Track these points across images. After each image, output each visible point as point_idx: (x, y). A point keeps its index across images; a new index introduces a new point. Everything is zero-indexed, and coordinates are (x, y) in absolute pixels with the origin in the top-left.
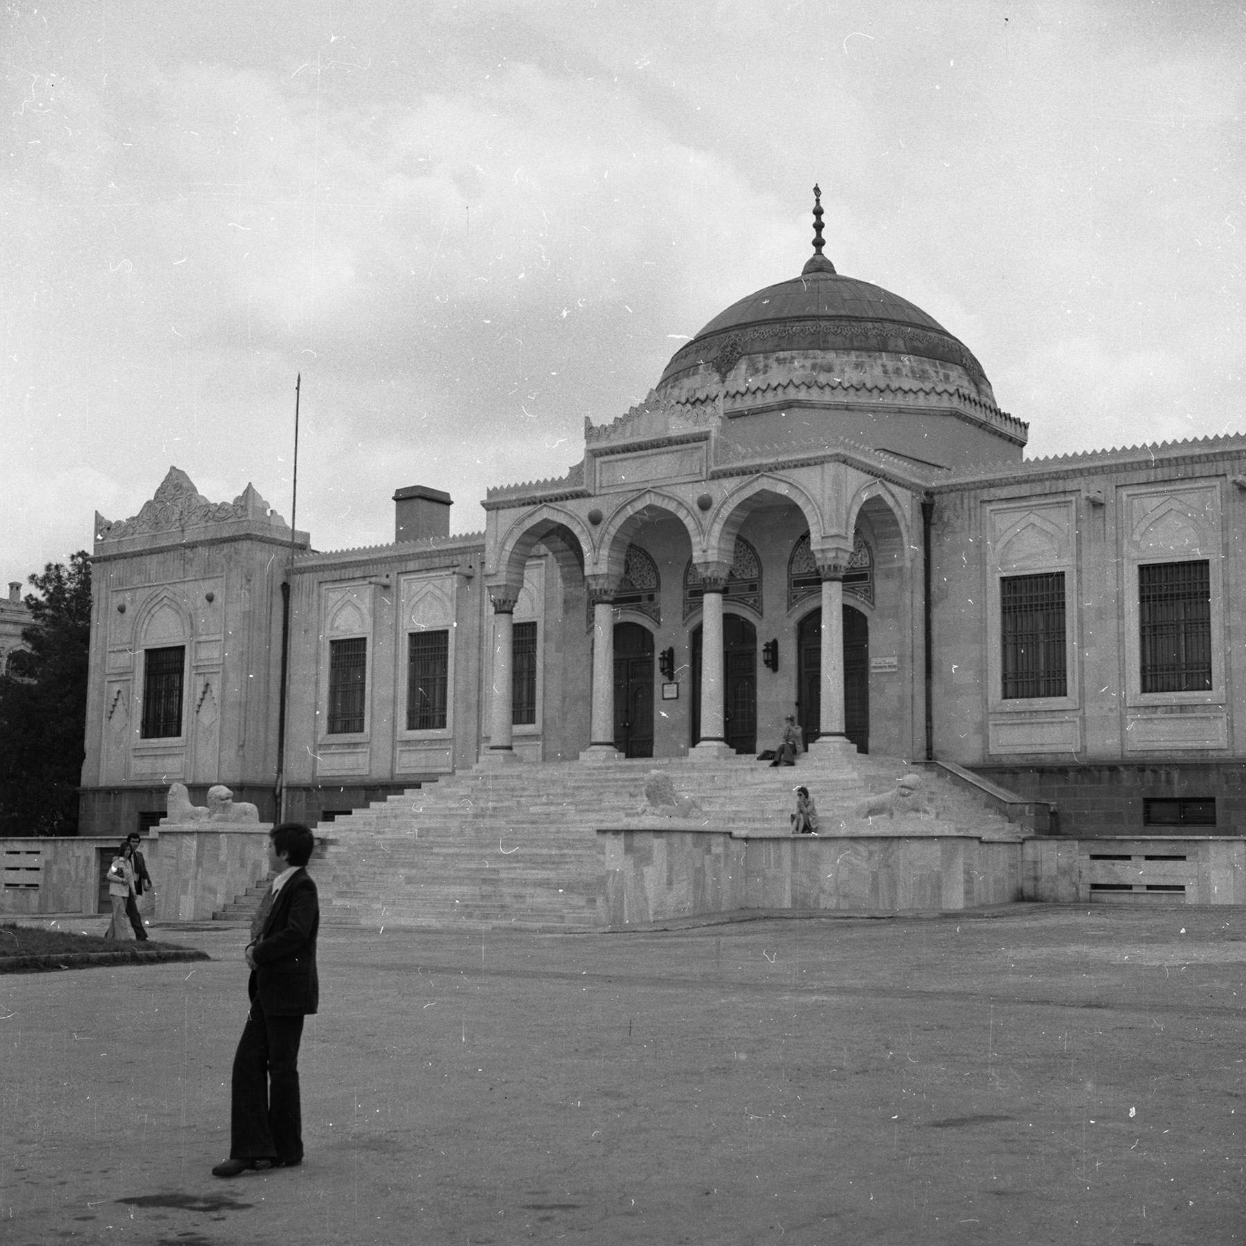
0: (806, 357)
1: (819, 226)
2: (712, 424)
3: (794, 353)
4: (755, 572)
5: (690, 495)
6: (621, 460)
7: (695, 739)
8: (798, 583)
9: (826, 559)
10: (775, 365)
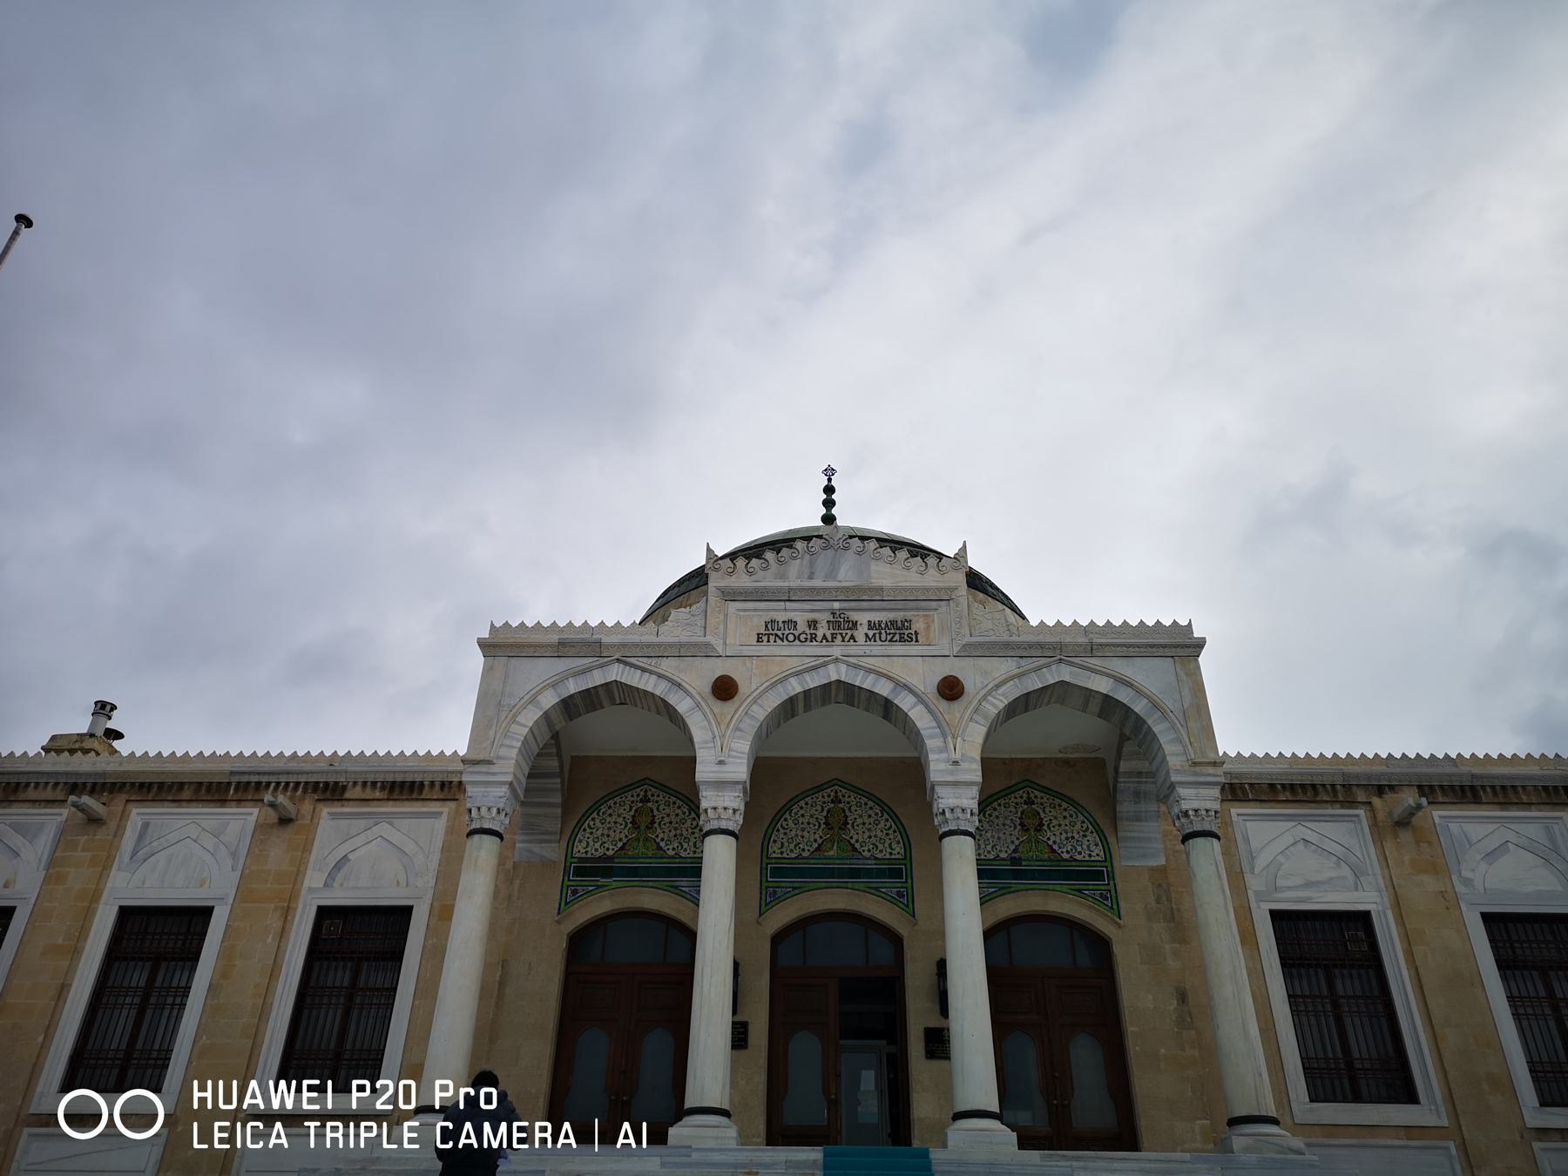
4: (898, 849)
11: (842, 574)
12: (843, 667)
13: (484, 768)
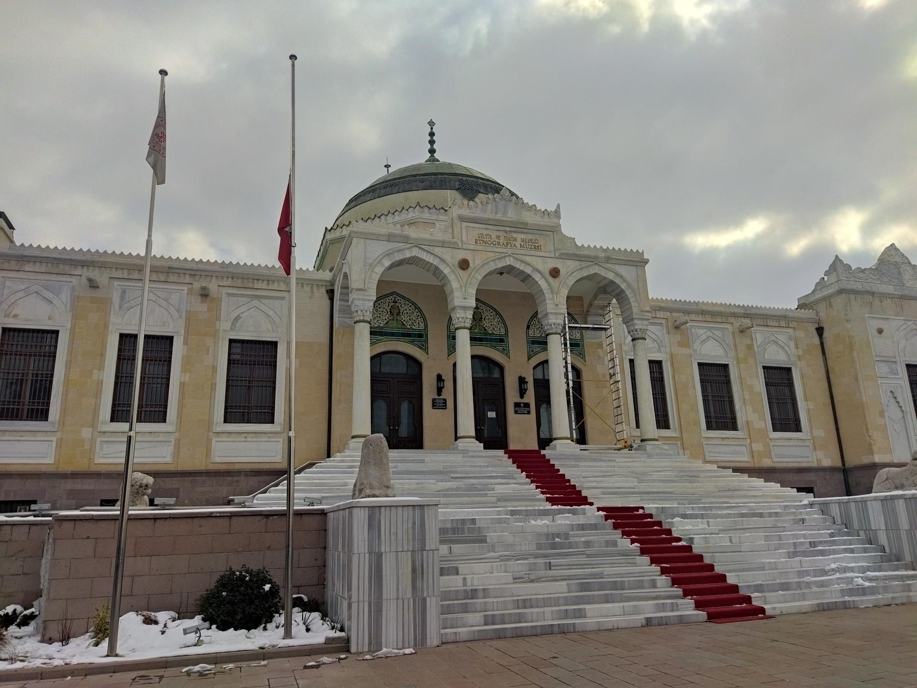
1: (432, 142)
4: (503, 330)
8: (533, 342)
11: (509, 215)
13: (362, 293)
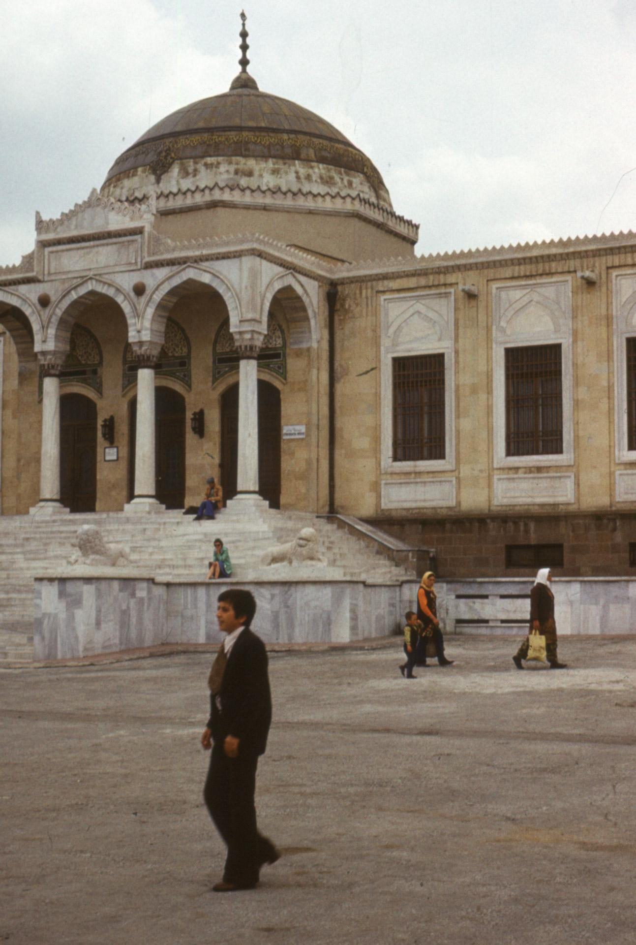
0: (230, 163)
2: (145, 219)
3: (220, 159)
4: (185, 350)
5: (127, 282)
6: (68, 250)
7: (131, 496)
8: (221, 361)
9: (243, 339)
10: (202, 168)
12: (94, 282)
